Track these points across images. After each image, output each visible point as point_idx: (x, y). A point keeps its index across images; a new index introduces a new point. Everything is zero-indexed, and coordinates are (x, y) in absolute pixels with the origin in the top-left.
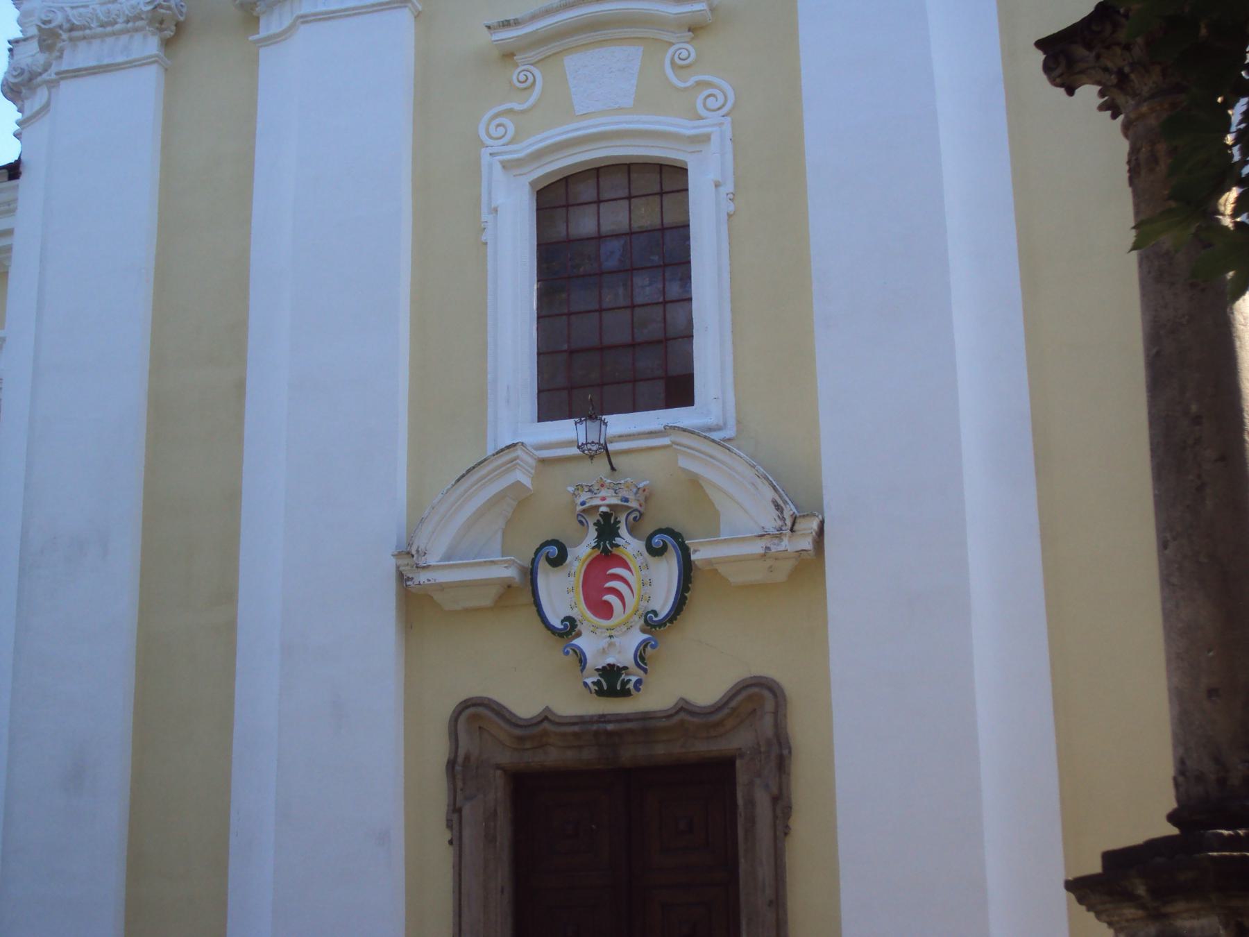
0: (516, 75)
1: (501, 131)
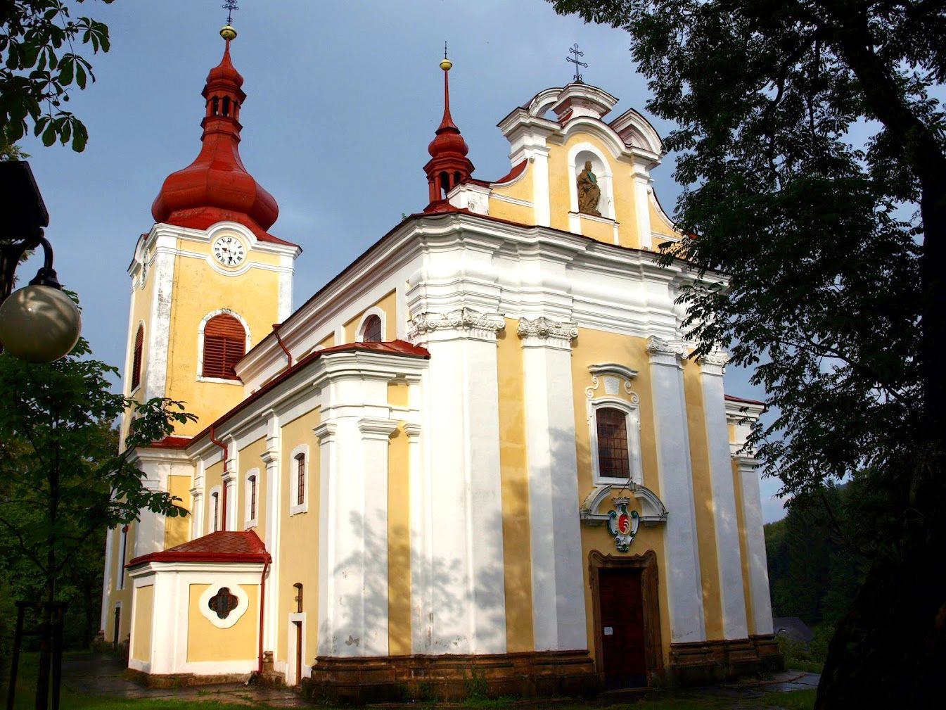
0: (593, 378)
1: (590, 394)
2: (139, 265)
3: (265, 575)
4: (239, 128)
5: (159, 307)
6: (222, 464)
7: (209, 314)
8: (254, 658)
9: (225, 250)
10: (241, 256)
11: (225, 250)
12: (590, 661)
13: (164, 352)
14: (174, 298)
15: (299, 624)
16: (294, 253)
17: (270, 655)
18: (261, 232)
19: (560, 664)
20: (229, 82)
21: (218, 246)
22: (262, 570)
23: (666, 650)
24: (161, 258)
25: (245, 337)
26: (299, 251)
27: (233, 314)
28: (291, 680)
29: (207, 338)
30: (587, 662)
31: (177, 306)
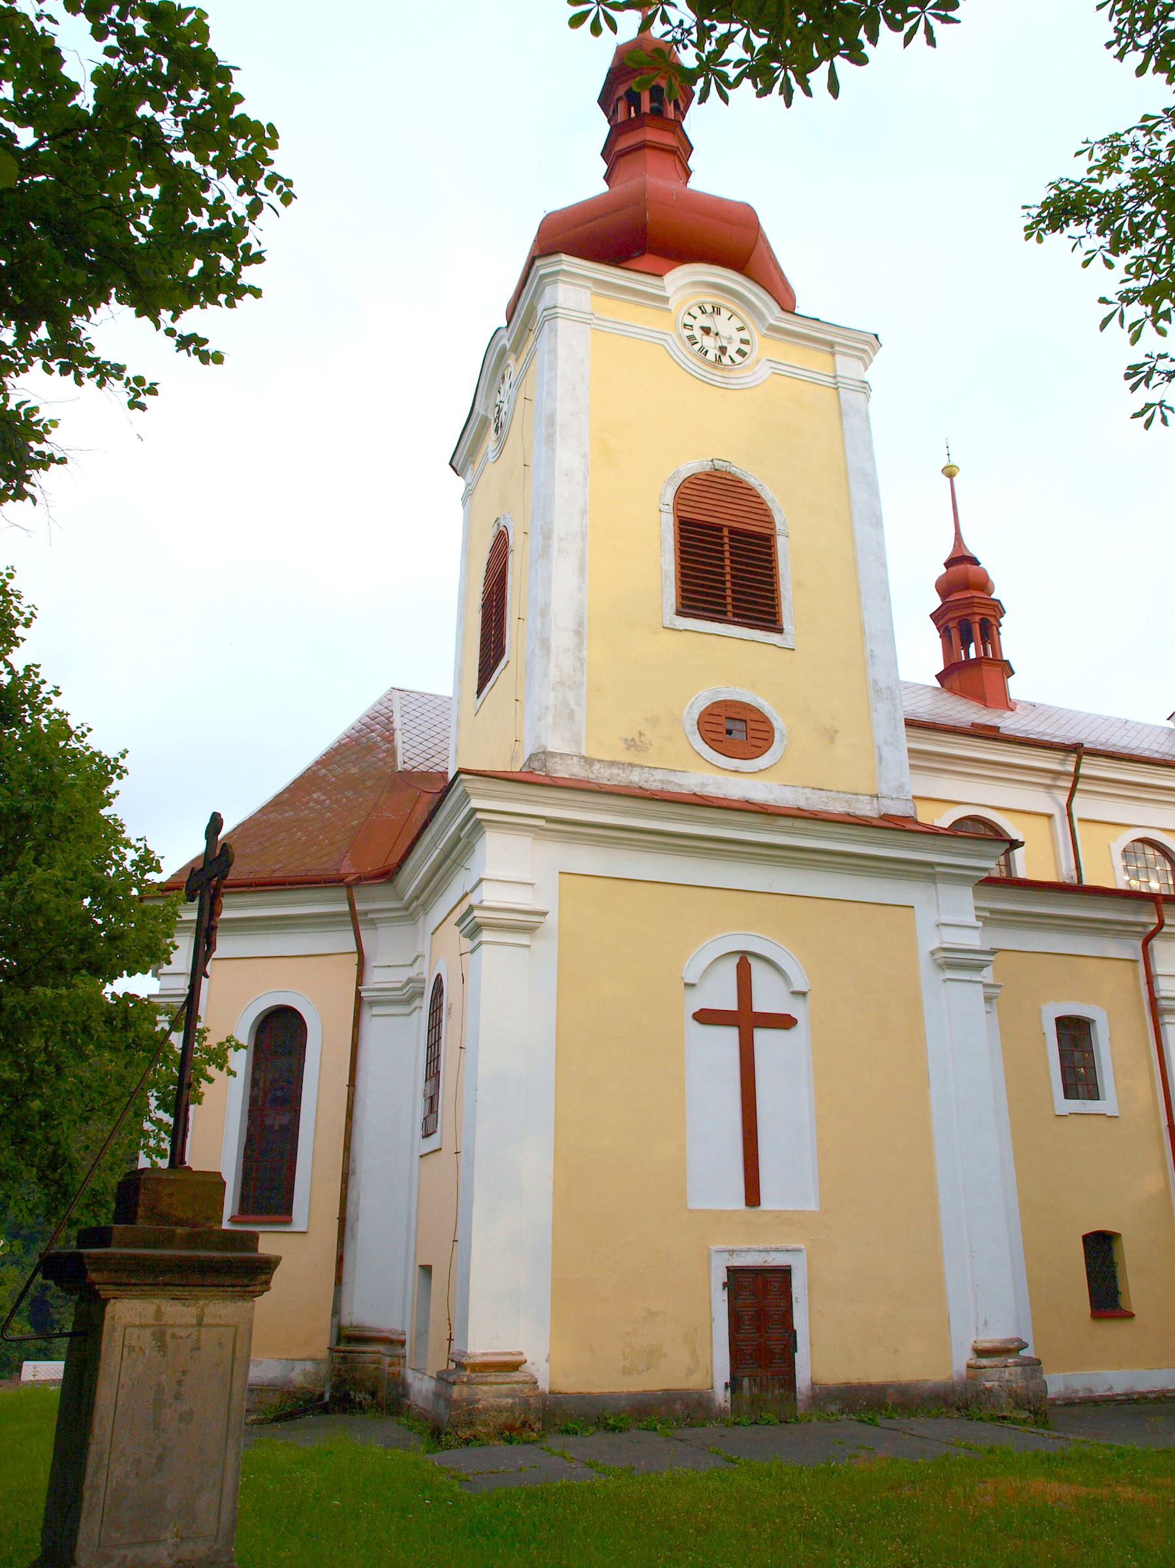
10: (745, 348)
11: (706, 331)
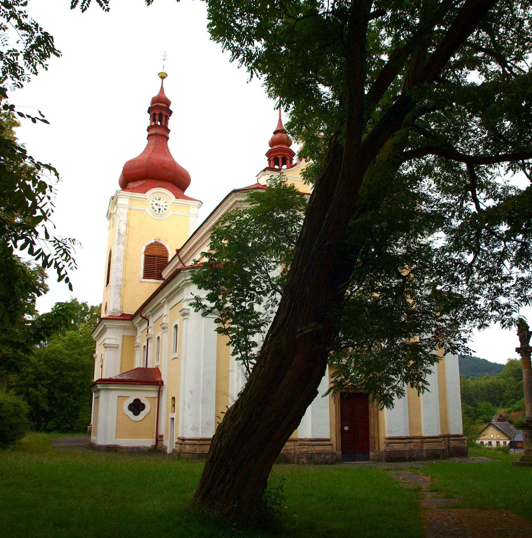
2: (111, 213)
3: (159, 392)
4: (169, 131)
5: (118, 239)
6: (147, 329)
7: (147, 243)
8: (153, 438)
9: (157, 204)
10: (166, 208)
11: (157, 204)
12: (332, 445)
13: (121, 265)
14: (127, 233)
15: (173, 419)
16: (198, 205)
17: (162, 436)
18: (179, 192)
19: (312, 445)
20: (162, 105)
21: (152, 203)
22: (158, 389)
23: (382, 441)
24: (120, 210)
25: (168, 255)
26: (201, 204)
27: (162, 242)
28: (169, 451)
29: (146, 256)
30: (329, 445)
31: (128, 238)
